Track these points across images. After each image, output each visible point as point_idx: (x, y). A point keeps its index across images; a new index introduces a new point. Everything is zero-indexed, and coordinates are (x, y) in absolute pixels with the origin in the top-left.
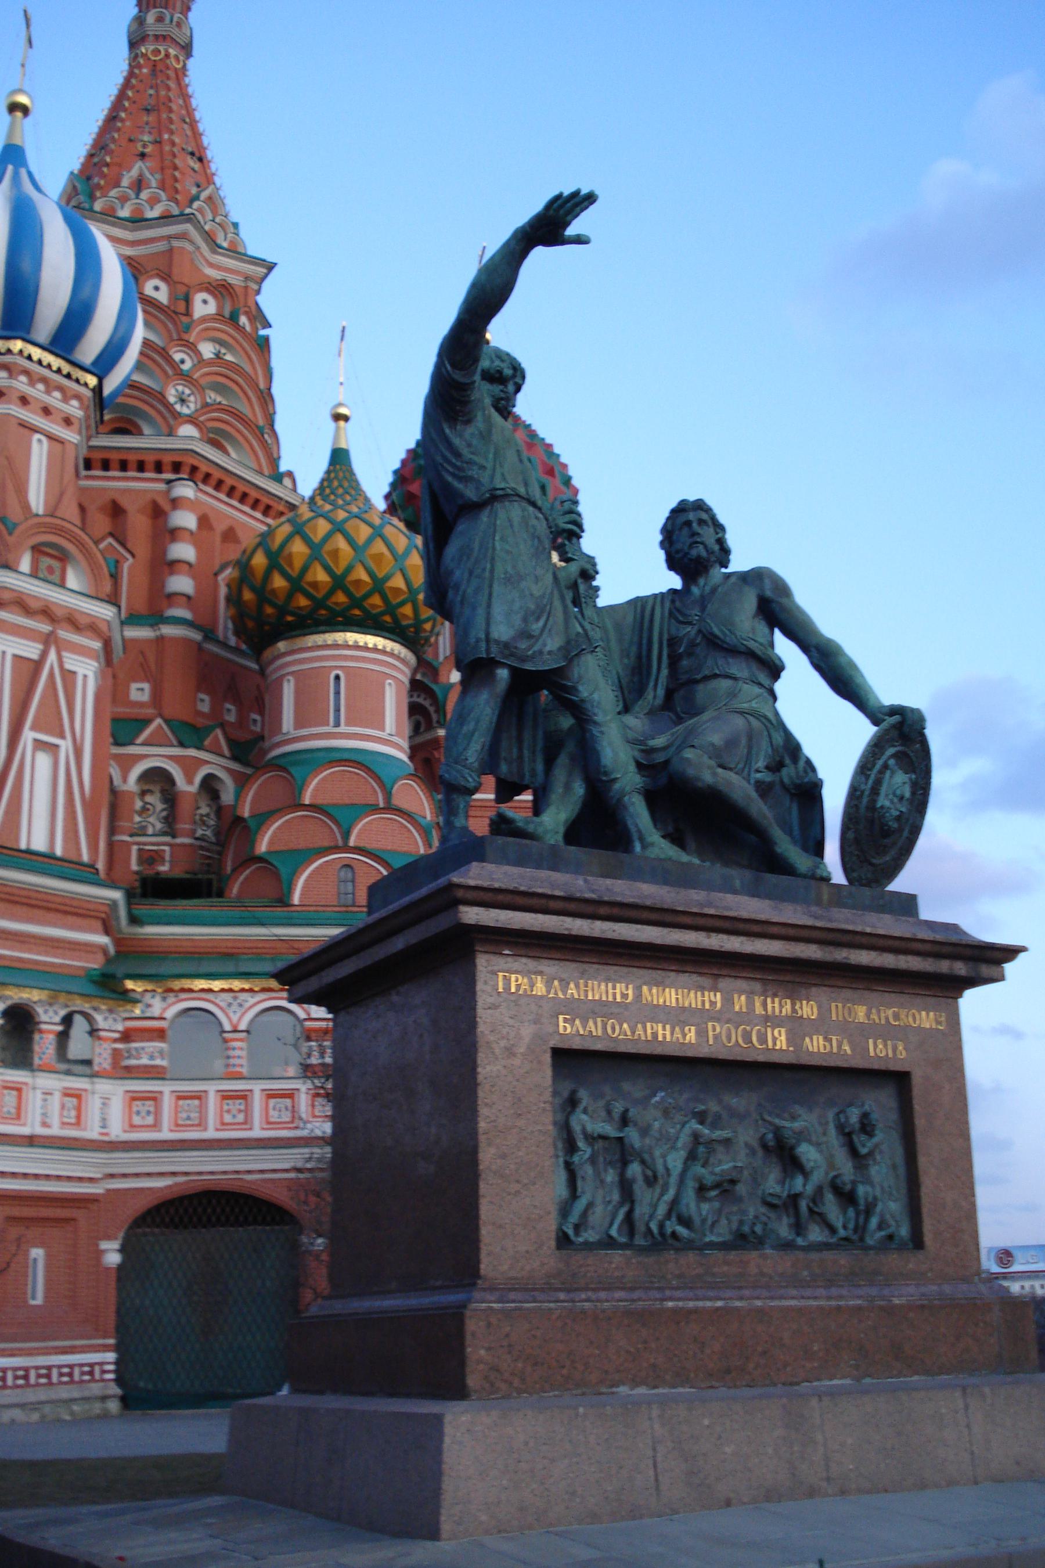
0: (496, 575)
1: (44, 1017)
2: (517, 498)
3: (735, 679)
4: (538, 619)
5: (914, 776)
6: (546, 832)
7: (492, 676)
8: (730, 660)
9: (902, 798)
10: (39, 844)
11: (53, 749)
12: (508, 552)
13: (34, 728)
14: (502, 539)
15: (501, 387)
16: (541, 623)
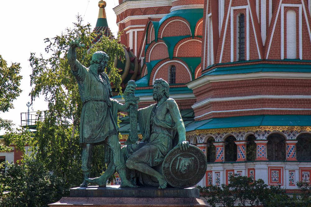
0: (84, 122)
1: (288, 138)
2: (92, 101)
3: (157, 133)
4: (99, 129)
5: (193, 158)
6: (99, 181)
7: (86, 146)
8: (157, 128)
9: (185, 166)
10: (291, 55)
11: (296, 10)
12: (87, 116)
13: (283, 3)
14: (86, 113)
15: (98, 65)
16: (99, 130)
